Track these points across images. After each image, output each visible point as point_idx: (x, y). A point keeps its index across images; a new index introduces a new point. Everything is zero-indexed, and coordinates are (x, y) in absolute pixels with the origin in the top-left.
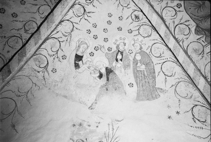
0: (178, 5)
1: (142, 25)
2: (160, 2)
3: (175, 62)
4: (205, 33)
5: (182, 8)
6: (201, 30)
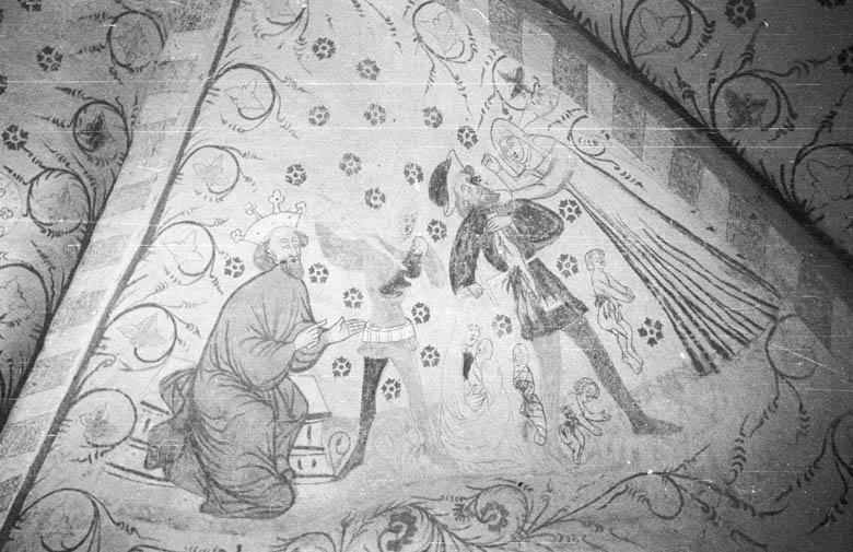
0: (234, 263)
1: (77, 177)
2: (209, 194)
3: (7, 387)
4: (181, 411)
5: (229, 284)
6: (184, 392)
